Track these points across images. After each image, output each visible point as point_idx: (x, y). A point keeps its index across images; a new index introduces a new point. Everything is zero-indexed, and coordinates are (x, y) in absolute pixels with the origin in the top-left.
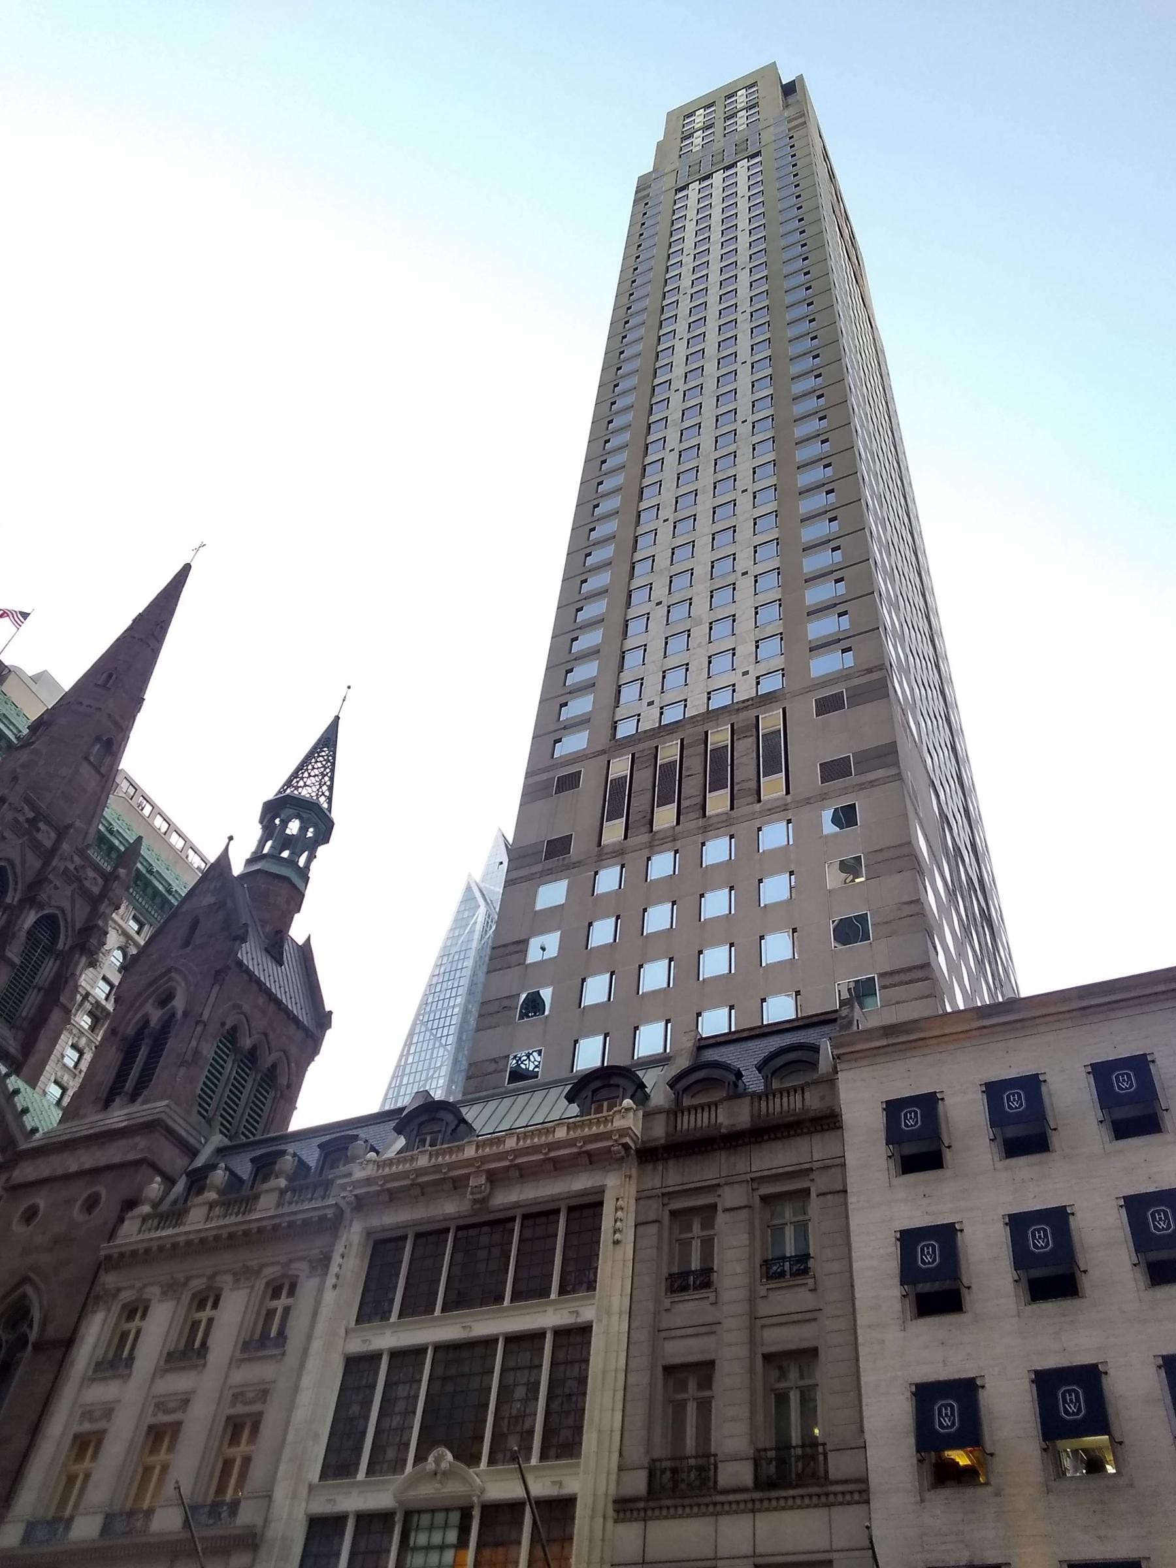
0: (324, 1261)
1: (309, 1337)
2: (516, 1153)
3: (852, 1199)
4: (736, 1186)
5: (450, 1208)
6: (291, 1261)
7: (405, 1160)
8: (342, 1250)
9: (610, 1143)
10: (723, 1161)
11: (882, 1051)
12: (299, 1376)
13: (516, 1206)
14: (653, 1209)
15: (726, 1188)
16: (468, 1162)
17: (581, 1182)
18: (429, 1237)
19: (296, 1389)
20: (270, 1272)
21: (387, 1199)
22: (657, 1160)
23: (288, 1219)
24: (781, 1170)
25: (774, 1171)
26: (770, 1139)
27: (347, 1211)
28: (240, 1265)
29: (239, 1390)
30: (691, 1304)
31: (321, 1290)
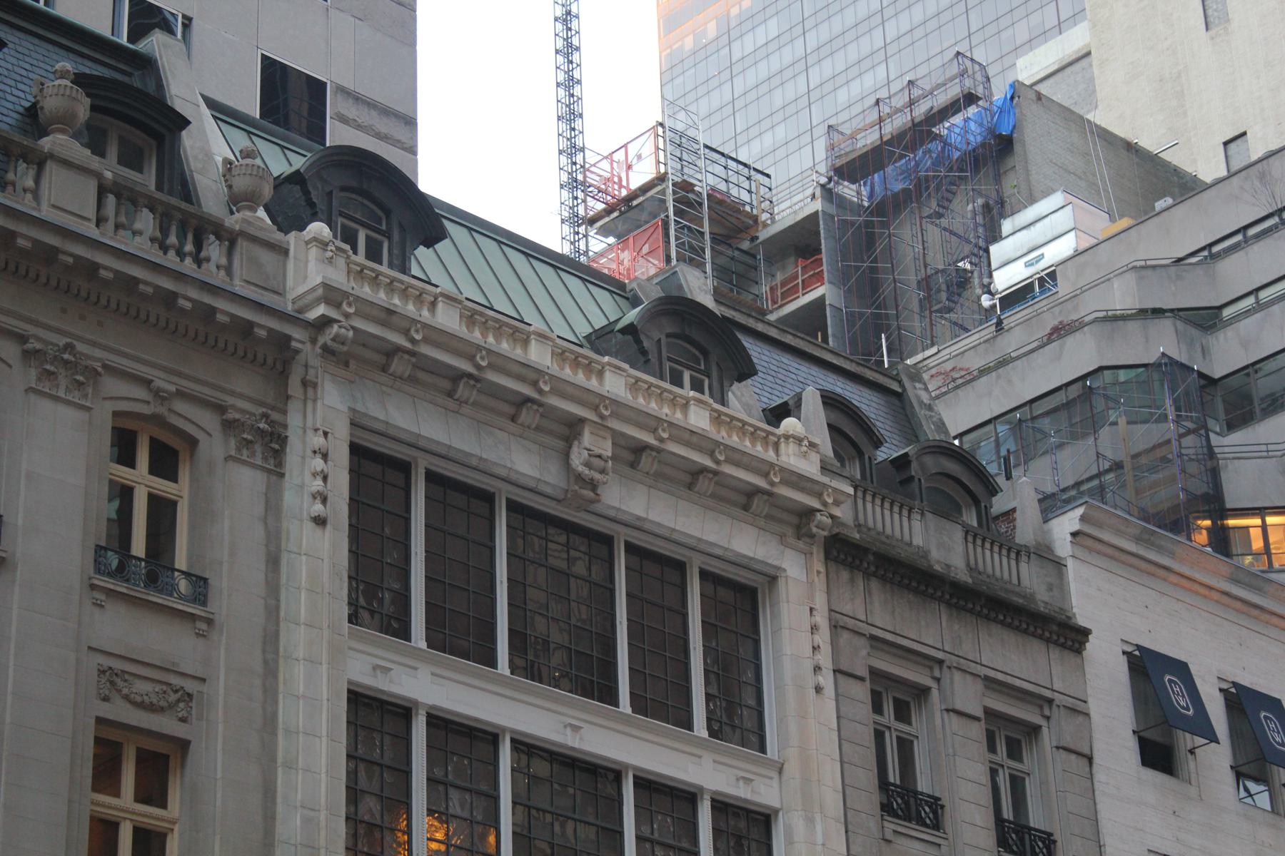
0: (273, 444)
1: (273, 613)
2: (439, 337)
3: (1100, 776)
4: (968, 677)
5: (521, 462)
6: (181, 394)
7: (576, 363)
8: (318, 441)
9: (815, 504)
10: (944, 624)
11: (1124, 557)
12: (270, 693)
13: (636, 525)
14: (862, 659)
15: (957, 676)
16: (597, 401)
17: (746, 542)
18: (462, 498)
19: (270, 723)
20: (123, 395)
21: (406, 375)
22: (858, 568)
23: (194, 293)
24: (1018, 683)
25: (1009, 680)
26: (1002, 623)
27: (309, 352)
28: (63, 341)
29: (118, 665)
30: (917, 845)
31: (272, 507)
